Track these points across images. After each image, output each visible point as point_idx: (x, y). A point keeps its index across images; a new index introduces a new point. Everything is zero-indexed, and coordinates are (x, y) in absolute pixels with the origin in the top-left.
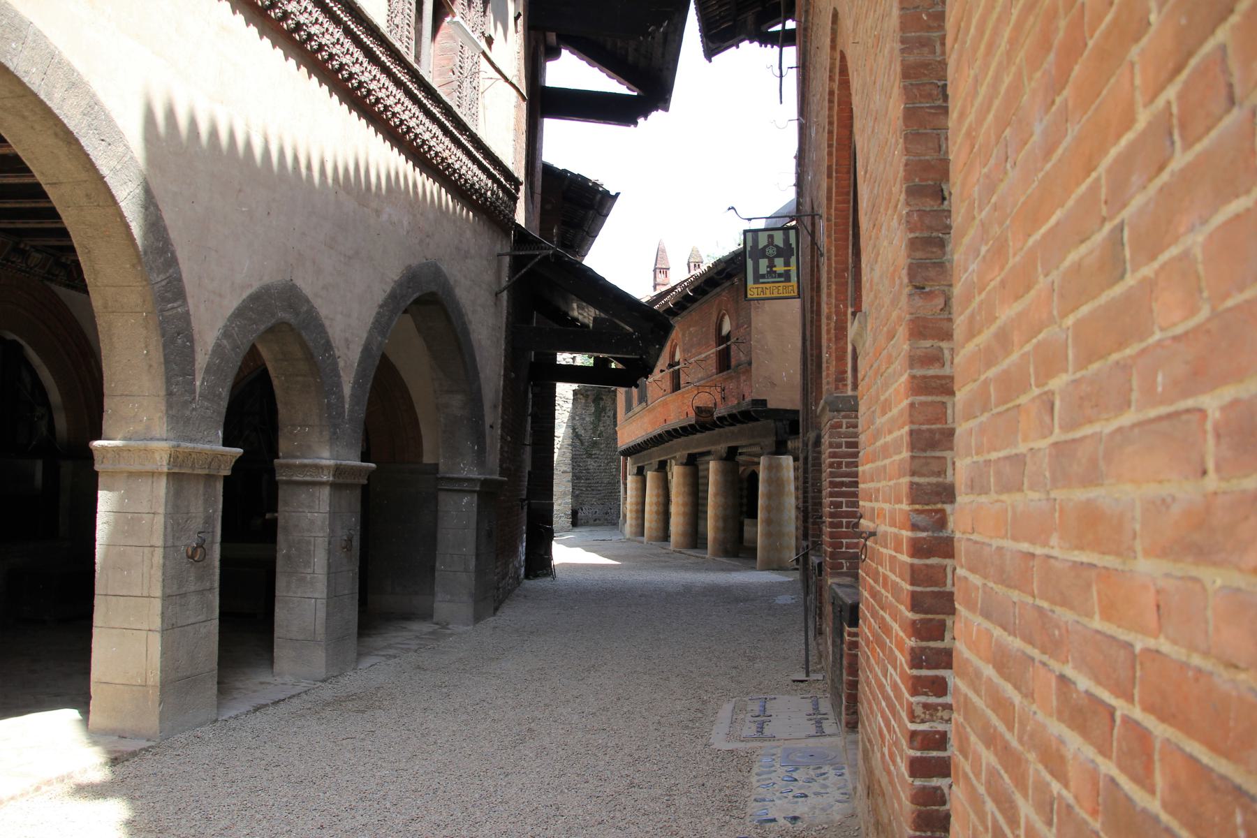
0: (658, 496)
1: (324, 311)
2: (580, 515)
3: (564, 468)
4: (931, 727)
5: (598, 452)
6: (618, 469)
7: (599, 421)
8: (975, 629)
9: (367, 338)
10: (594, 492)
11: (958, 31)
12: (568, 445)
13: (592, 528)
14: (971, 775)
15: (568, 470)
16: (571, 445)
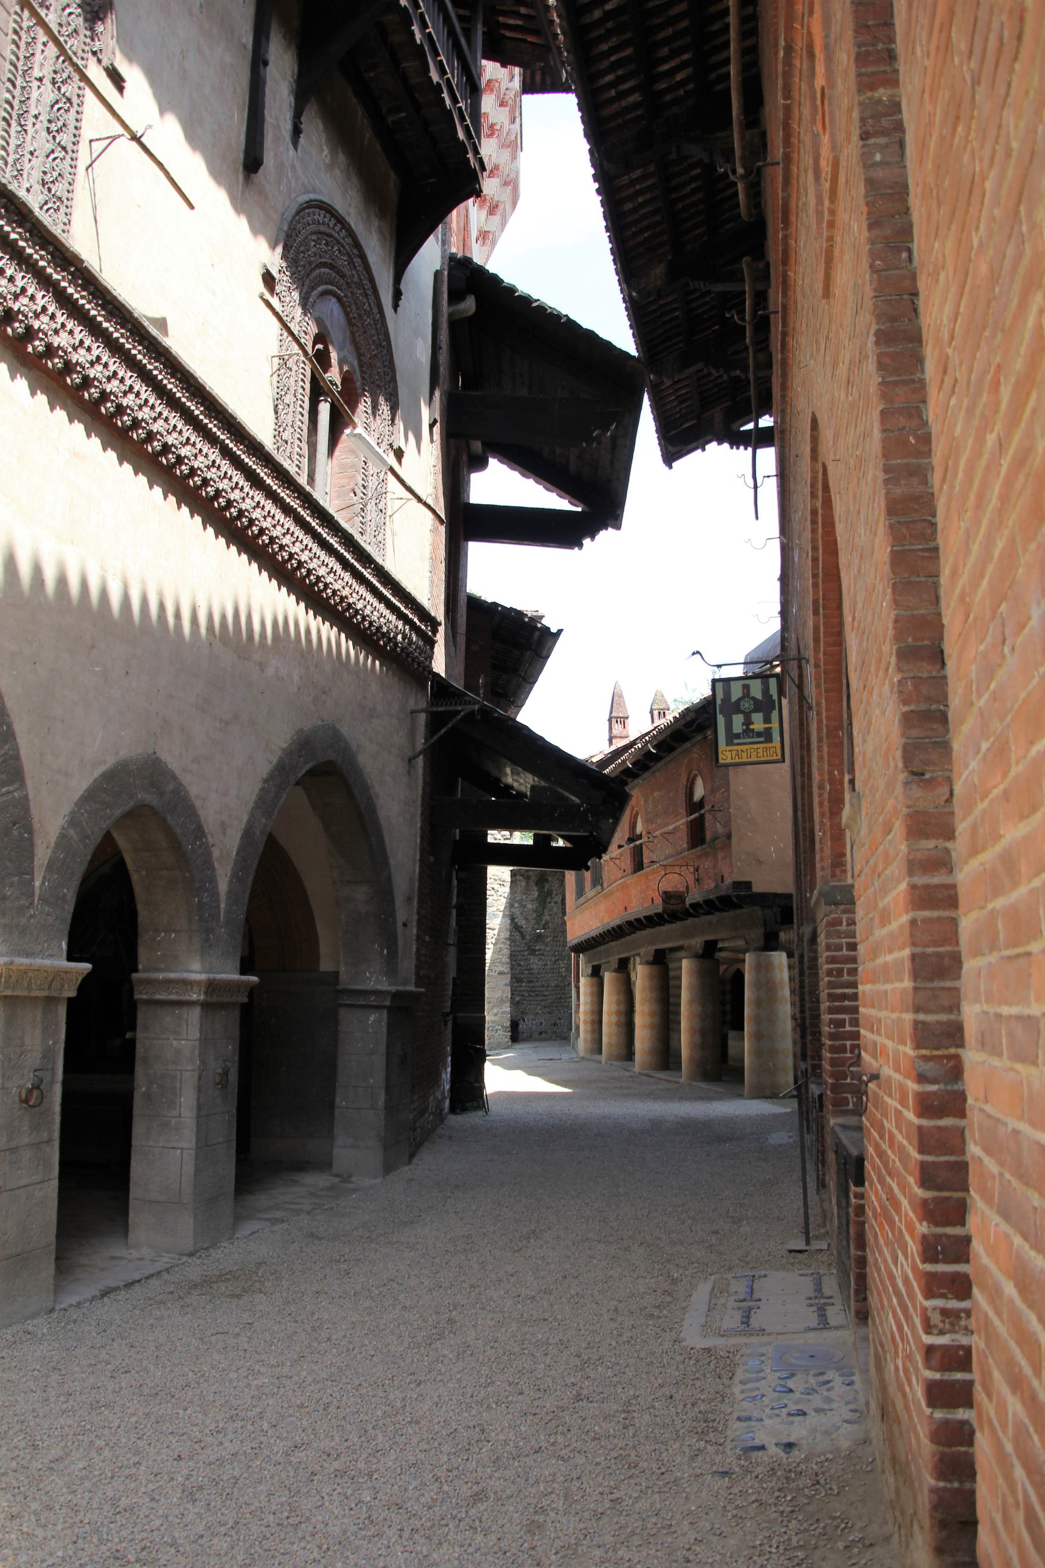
0: (618, 1003)
1: (194, 788)
2: (522, 1027)
3: (500, 968)
4: (953, 1340)
5: (543, 948)
6: (568, 969)
7: (544, 908)
8: (992, 1230)
9: (248, 822)
10: (539, 998)
11: (946, 470)
12: (506, 939)
13: (537, 1044)
14: (996, 1424)
15: (506, 971)
16: (509, 939)
